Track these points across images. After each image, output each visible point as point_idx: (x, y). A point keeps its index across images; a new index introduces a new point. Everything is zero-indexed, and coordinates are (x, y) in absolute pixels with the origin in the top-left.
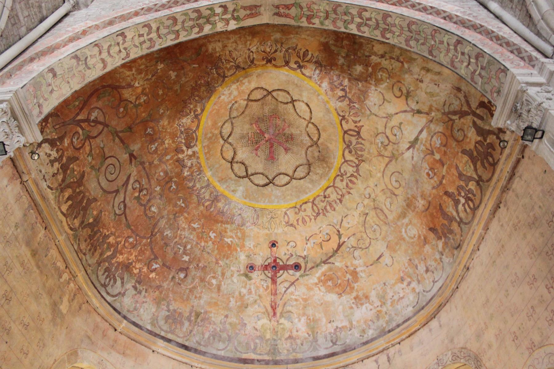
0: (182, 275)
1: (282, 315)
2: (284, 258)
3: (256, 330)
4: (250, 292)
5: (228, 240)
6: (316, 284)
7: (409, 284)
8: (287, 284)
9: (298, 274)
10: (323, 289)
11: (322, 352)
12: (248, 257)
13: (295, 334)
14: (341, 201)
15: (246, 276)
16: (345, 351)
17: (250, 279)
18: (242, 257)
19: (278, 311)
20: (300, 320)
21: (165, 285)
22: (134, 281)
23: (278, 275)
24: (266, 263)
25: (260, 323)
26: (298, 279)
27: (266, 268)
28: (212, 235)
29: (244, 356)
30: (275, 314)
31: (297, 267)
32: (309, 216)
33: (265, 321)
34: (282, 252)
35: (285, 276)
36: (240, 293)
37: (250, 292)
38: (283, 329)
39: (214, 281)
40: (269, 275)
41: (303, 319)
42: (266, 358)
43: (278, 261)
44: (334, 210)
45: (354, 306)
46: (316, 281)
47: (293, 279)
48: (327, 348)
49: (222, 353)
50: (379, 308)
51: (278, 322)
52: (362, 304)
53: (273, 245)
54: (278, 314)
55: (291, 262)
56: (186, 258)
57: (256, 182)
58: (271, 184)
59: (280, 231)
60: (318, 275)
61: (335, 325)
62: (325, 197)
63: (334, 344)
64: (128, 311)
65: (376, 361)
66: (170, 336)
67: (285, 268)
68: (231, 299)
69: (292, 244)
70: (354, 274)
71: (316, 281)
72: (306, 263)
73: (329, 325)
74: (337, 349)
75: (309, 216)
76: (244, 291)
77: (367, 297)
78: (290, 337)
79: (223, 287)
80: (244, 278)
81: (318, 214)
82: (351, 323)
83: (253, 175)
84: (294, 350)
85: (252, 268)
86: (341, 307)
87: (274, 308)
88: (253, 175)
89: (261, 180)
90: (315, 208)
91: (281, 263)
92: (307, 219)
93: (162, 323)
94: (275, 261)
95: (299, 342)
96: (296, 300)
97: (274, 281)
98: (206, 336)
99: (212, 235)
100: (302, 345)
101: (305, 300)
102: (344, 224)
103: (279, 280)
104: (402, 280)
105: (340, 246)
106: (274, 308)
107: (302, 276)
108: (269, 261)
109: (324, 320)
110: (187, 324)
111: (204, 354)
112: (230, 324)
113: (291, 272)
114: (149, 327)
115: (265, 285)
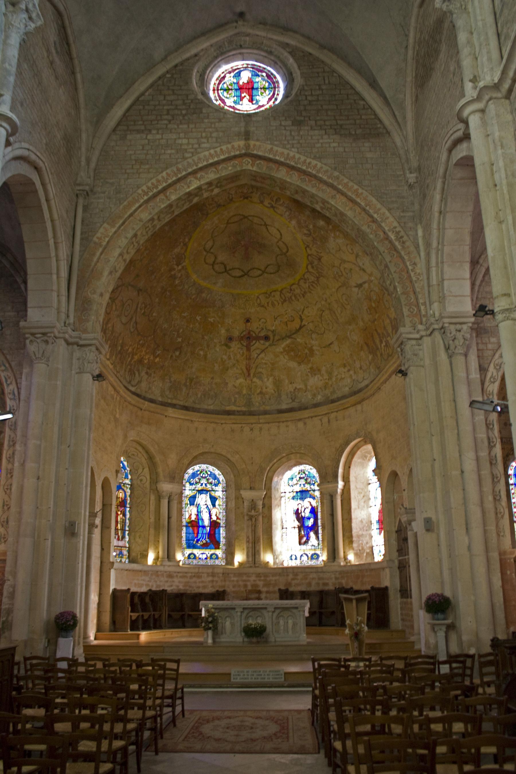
0: (177, 353)
1: (254, 376)
2: (257, 331)
3: (235, 387)
4: (230, 358)
5: (211, 320)
6: (282, 353)
7: (349, 371)
8: (258, 352)
9: (267, 344)
10: (286, 357)
11: (284, 407)
12: (227, 330)
13: (264, 390)
14: (304, 296)
15: (226, 345)
16: (300, 409)
17: (229, 347)
18: (223, 331)
19: (252, 372)
20: (268, 380)
21: (166, 364)
22: (145, 369)
23: (252, 344)
24: (242, 335)
25: (238, 382)
26: (267, 348)
27: (241, 338)
28: (198, 318)
29: (228, 408)
30: (249, 375)
31: (267, 338)
32: (277, 301)
33: (241, 380)
34: (255, 326)
35: (258, 345)
36: (222, 359)
37: (230, 358)
38: (256, 386)
39: (202, 353)
40: (245, 344)
41: (271, 379)
42: (244, 409)
43: (251, 333)
44: (298, 300)
45: (309, 374)
46: (282, 350)
47: (263, 347)
48: (287, 404)
49: (212, 407)
50: (327, 381)
51: (252, 380)
52: (315, 375)
53: (248, 321)
54: (252, 375)
55: (262, 334)
56: (180, 340)
57: (234, 274)
58: (246, 276)
59: (253, 310)
60: (283, 346)
61: (294, 385)
62: (291, 290)
63: (293, 401)
64: (146, 392)
65: (321, 420)
66: (174, 402)
67: (258, 338)
68: (216, 364)
69: (263, 320)
70: (311, 350)
71: (282, 350)
72: (274, 336)
73: (290, 386)
74: (295, 405)
75: (277, 301)
76: (225, 357)
77: (319, 370)
78: (261, 393)
79: (209, 356)
80: (224, 347)
81: (285, 301)
82: (306, 386)
83: (230, 270)
84: (264, 403)
85: (230, 339)
86: (299, 373)
87: (248, 370)
88: (230, 270)
89: (238, 273)
90: (282, 295)
91: (254, 335)
92: (276, 303)
93: (167, 393)
94: (249, 333)
95: (267, 397)
96: (266, 364)
97: (248, 349)
98: (199, 396)
99: (198, 318)
100: (270, 399)
101: (273, 364)
102: (306, 312)
103: (252, 348)
104: (345, 366)
105: (301, 327)
106: (248, 370)
107: (270, 345)
108: (244, 333)
109: (287, 381)
110: (184, 389)
111: (197, 410)
112: (216, 384)
113: (262, 342)
114: (160, 399)
115: (241, 352)
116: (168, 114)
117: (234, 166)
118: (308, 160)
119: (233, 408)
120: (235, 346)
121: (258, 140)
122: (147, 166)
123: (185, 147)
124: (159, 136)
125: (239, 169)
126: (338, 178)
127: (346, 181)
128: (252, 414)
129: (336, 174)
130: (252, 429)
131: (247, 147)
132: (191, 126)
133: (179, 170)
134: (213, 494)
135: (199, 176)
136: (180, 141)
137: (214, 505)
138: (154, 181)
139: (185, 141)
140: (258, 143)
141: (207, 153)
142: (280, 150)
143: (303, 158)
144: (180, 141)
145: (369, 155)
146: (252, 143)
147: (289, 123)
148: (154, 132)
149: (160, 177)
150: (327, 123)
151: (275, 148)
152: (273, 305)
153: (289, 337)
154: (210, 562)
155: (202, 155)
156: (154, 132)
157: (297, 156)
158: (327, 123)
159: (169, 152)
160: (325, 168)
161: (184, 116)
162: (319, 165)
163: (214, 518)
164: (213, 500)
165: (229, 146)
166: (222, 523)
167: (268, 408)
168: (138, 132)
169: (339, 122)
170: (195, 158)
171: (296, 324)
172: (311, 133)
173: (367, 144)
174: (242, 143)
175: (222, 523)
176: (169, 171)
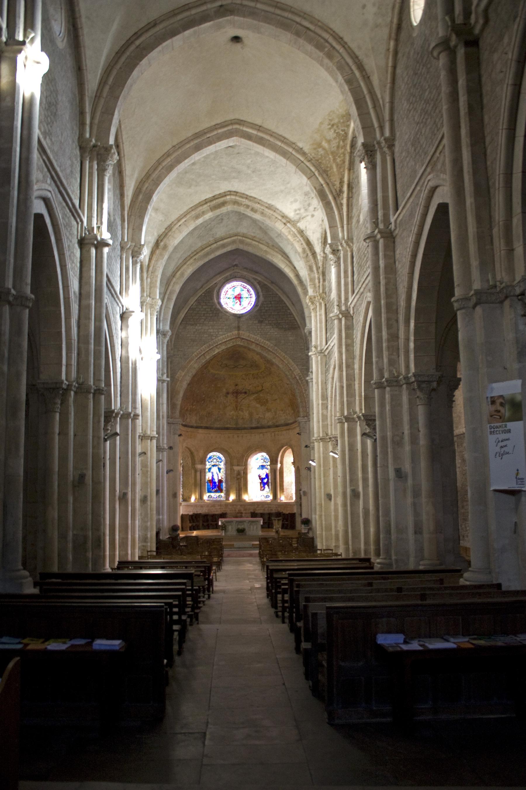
8: (241, 399)
9: (246, 395)
19: (239, 408)
25: (232, 413)
27: (233, 393)
29: (226, 426)
30: (237, 409)
31: (245, 393)
33: (233, 412)
34: (240, 387)
41: (247, 412)
42: (234, 426)
47: (244, 397)
53: (236, 385)
55: (244, 391)
67: (241, 393)
78: (243, 418)
85: (228, 393)
87: (237, 408)
97: (236, 397)
116: (204, 316)
117: (233, 343)
118: (265, 341)
119: (228, 426)
120: (230, 396)
121: (243, 331)
122: (196, 343)
123: (212, 334)
124: (200, 328)
125: (235, 344)
126: (276, 350)
127: (280, 351)
128: (238, 429)
129: (276, 348)
130: (238, 436)
131: (239, 334)
132: (215, 322)
133: (210, 345)
134: (219, 466)
135: (218, 347)
136: (210, 331)
137: (220, 472)
138: (199, 350)
139: (212, 331)
140: (243, 332)
141: (221, 337)
142: (253, 336)
143: (262, 340)
144: (210, 331)
145: (291, 338)
146: (241, 332)
147: (257, 322)
148: (198, 325)
149: (202, 348)
150: (273, 322)
151: (251, 335)
152: (249, 379)
153: (257, 393)
154: (218, 499)
155: (219, 338)
156: (198, 325)
157: (260, 339)
158: (273, 322)
159: (205, 336)
160: (272, 345)
161: (211, 317)
162: (269, 343)
163: (220, 478)
164: (219, 469)
165: (231, 333)
166: (224, 480)
167: (246, 426)
168: (192, 325)
169: (279, 322)
170: (217, 339)
171: (260, 388)
172: (267, 327)
173: (290, 333)
174: (236, 332)
175: (224, 480)
176: (205, 345)
